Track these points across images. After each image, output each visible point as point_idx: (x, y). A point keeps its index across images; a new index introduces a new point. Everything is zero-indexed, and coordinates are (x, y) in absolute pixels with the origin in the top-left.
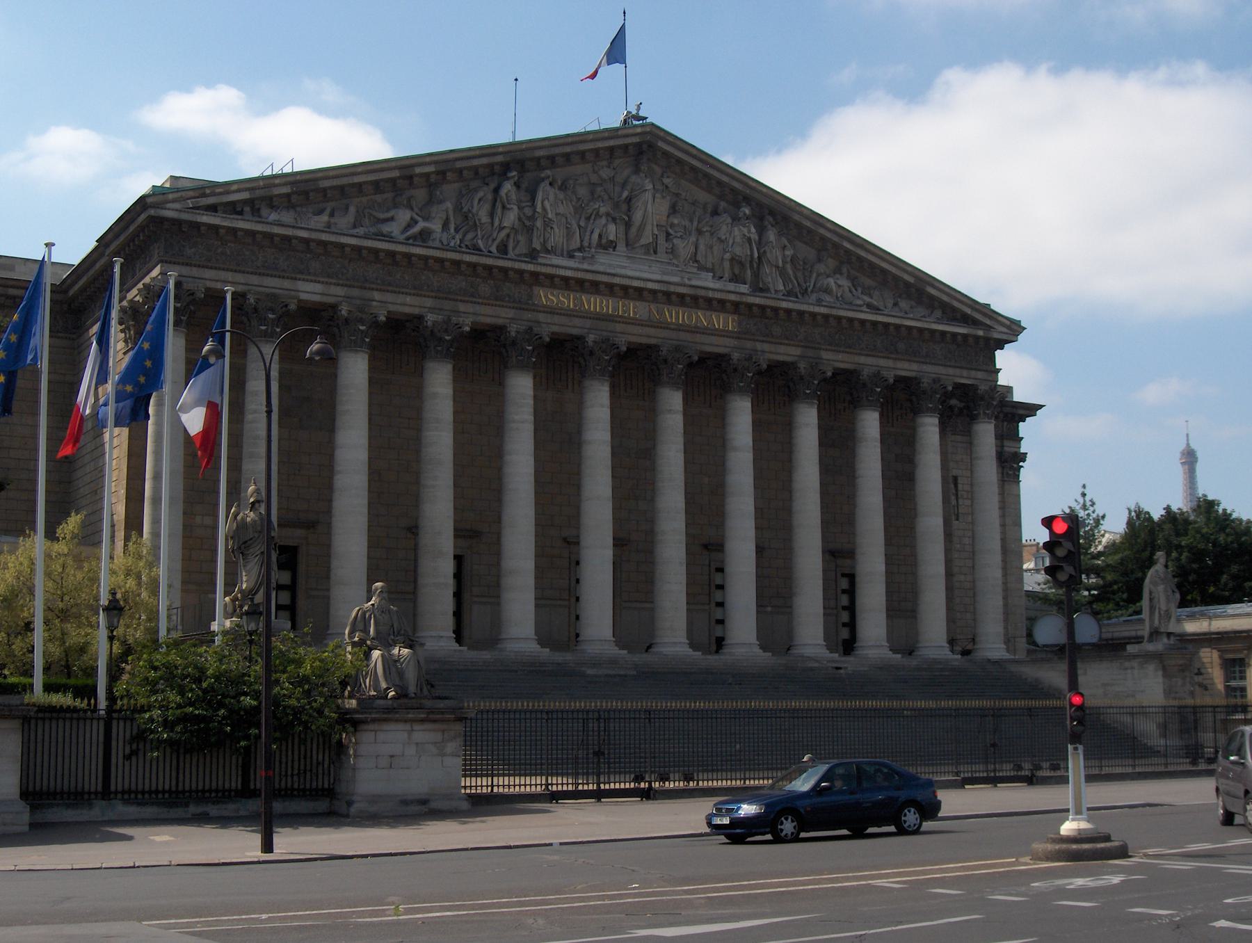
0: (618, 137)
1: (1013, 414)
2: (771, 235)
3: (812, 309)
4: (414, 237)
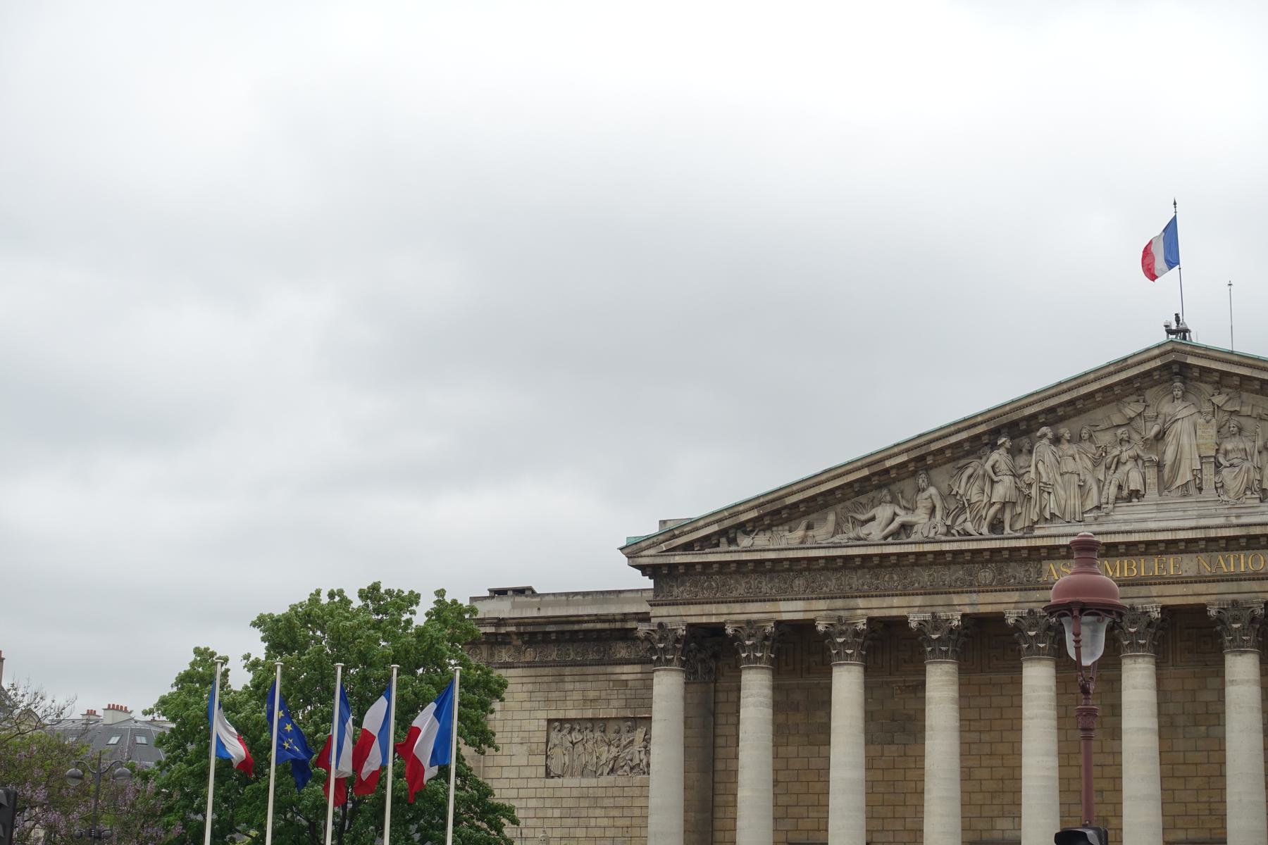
0: (1129, 367)
4: (892, 534)
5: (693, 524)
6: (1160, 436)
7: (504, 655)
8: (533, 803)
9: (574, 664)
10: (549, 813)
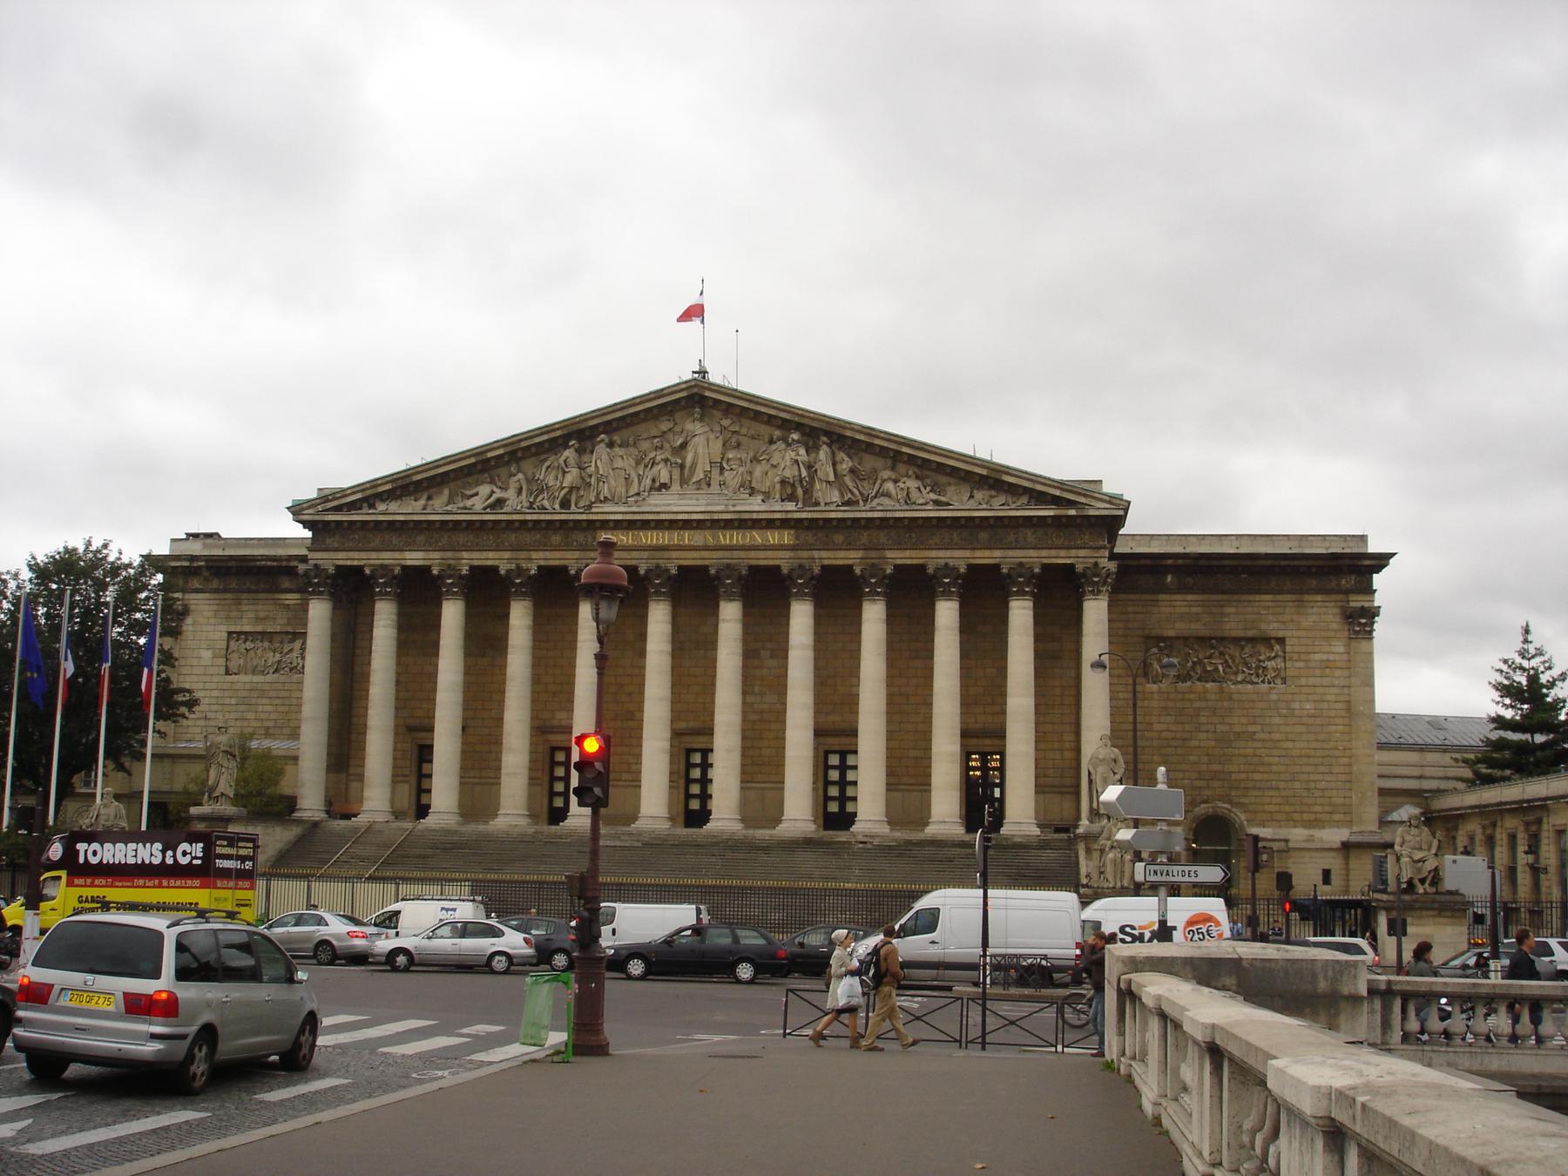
2: (824, 453)
3: (864, 515)
4: (492, 506)
5: (343, 492)
6: (684, 446)
7: (196, 584)
8: (215, 693)
9: (249, 591)
10: (227, 701)
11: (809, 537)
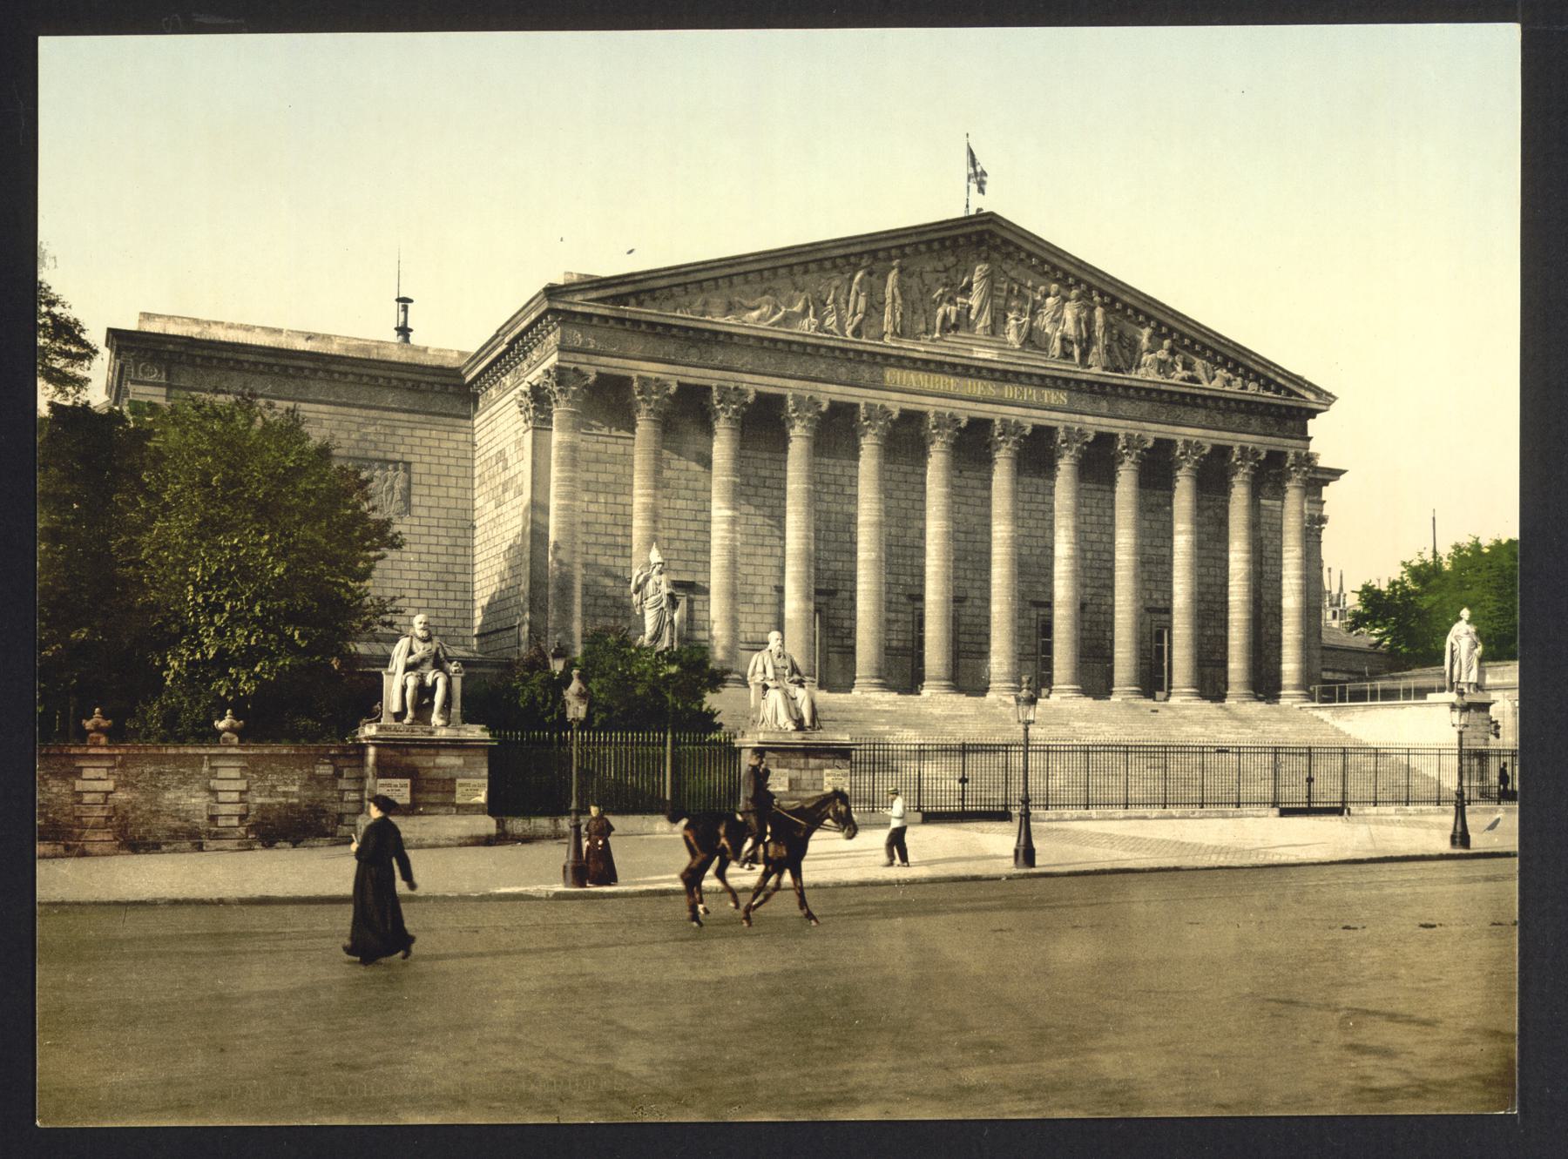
1: (1318, 479)
11: (1084, 402)
